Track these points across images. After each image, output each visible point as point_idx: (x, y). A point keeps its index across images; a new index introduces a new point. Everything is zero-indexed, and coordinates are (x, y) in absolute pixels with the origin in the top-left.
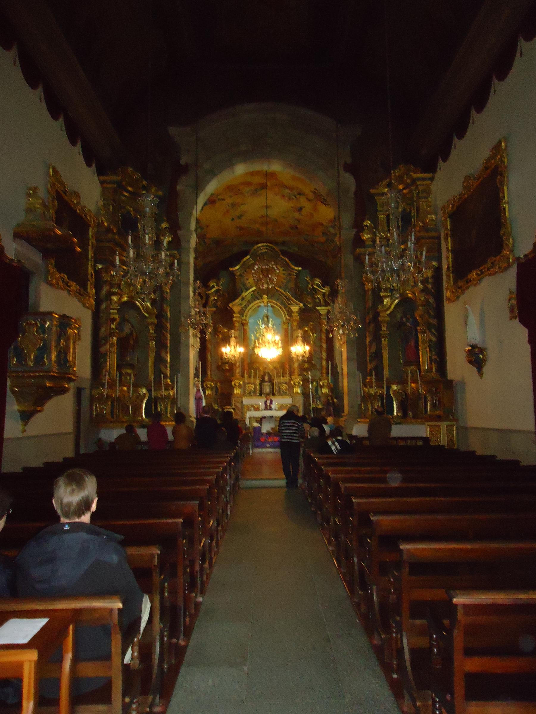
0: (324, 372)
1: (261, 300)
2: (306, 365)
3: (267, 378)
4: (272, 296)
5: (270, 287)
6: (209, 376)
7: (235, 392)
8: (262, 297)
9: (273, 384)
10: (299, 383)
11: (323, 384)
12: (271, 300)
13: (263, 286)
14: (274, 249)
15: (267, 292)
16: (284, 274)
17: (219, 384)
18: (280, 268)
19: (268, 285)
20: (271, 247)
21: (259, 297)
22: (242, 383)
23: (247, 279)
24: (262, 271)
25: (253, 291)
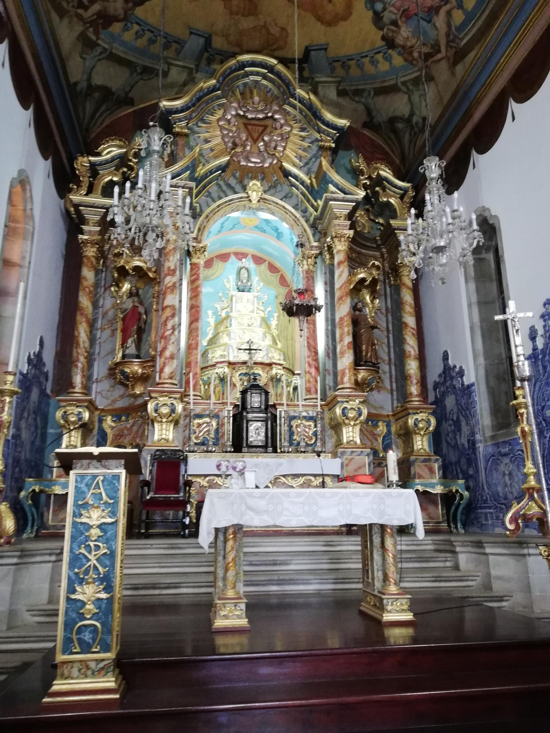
0: (414, 389)
1: (244, 195)
2: (362, 374)
3: (255, 400)
4: (270, 188)
5: (266, 165)
6: (77, 390)
7: (156, 437)
8: (244, 188)
9: (274, 417)
10: (360, 415)
11: (416, 425)
12: (266, 196)
13: (248, 160)
14: (278, 74)
15: (259, 173)
16: (303, 139)
17: (109, 421)
18: (292, 123)
19: (263, 162)
20: (271, 69)
21: (238, 188)
22: (179, 408)
23: (207, 141)
24: (246, 125)
25: (223, 168)
